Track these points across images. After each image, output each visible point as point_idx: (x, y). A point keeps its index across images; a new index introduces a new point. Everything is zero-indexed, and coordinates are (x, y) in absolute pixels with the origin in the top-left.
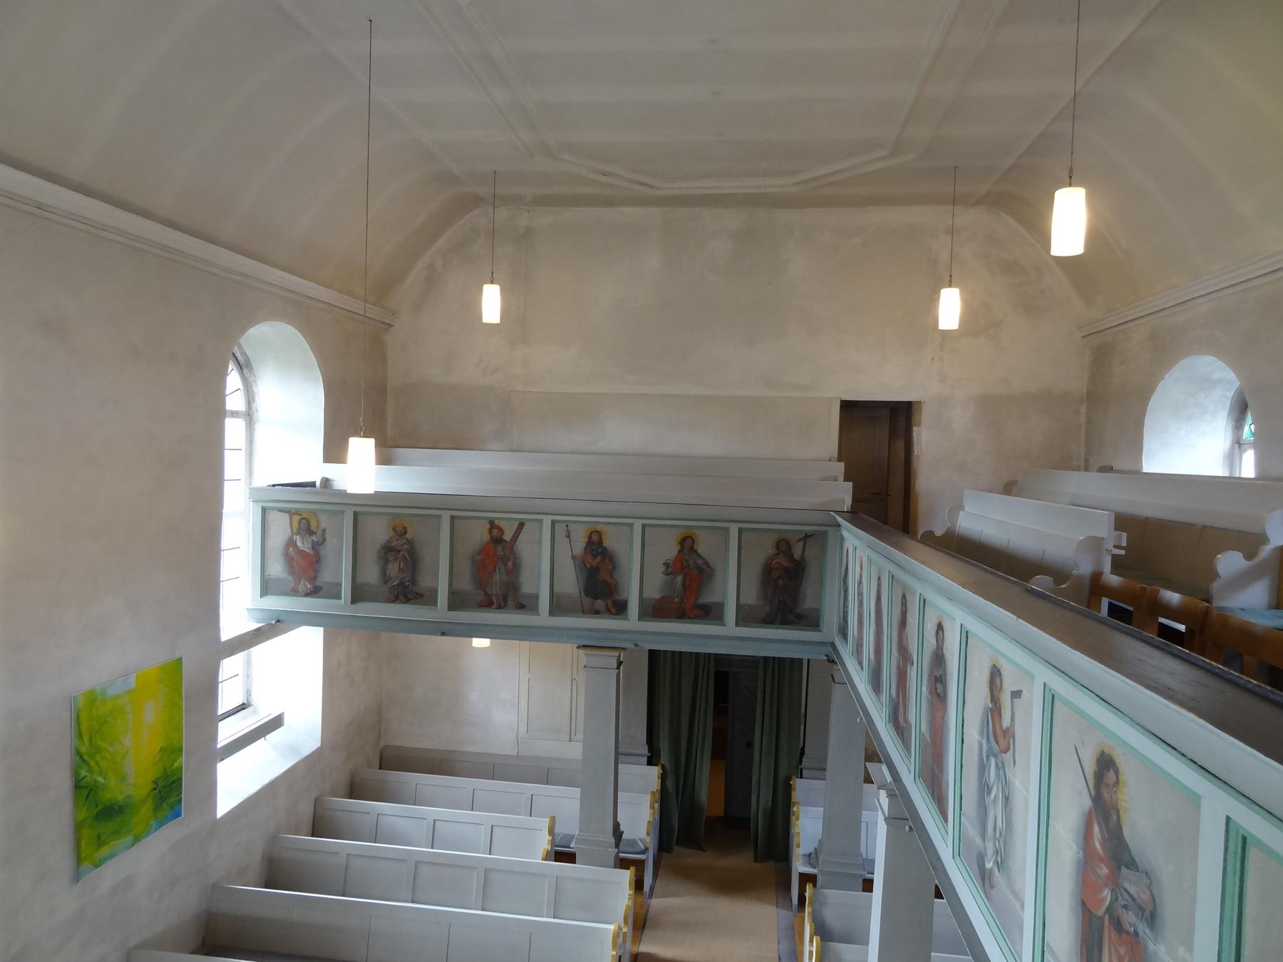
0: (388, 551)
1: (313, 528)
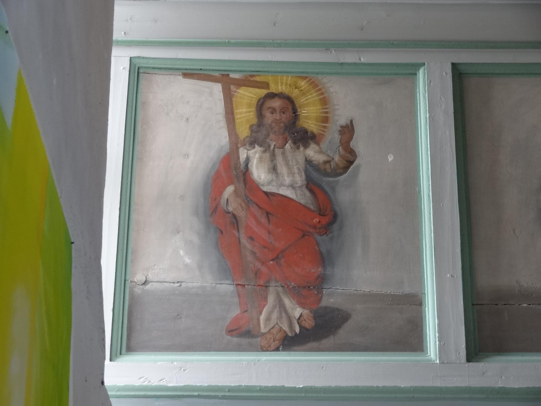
1: (309, 116)
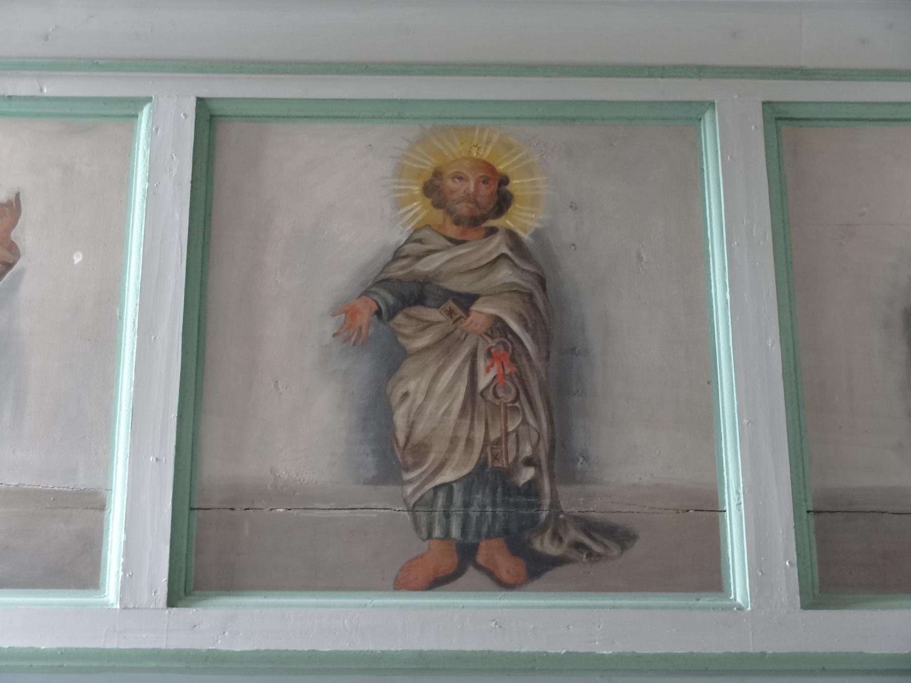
0: (398, 297)
